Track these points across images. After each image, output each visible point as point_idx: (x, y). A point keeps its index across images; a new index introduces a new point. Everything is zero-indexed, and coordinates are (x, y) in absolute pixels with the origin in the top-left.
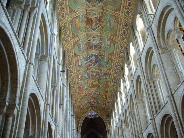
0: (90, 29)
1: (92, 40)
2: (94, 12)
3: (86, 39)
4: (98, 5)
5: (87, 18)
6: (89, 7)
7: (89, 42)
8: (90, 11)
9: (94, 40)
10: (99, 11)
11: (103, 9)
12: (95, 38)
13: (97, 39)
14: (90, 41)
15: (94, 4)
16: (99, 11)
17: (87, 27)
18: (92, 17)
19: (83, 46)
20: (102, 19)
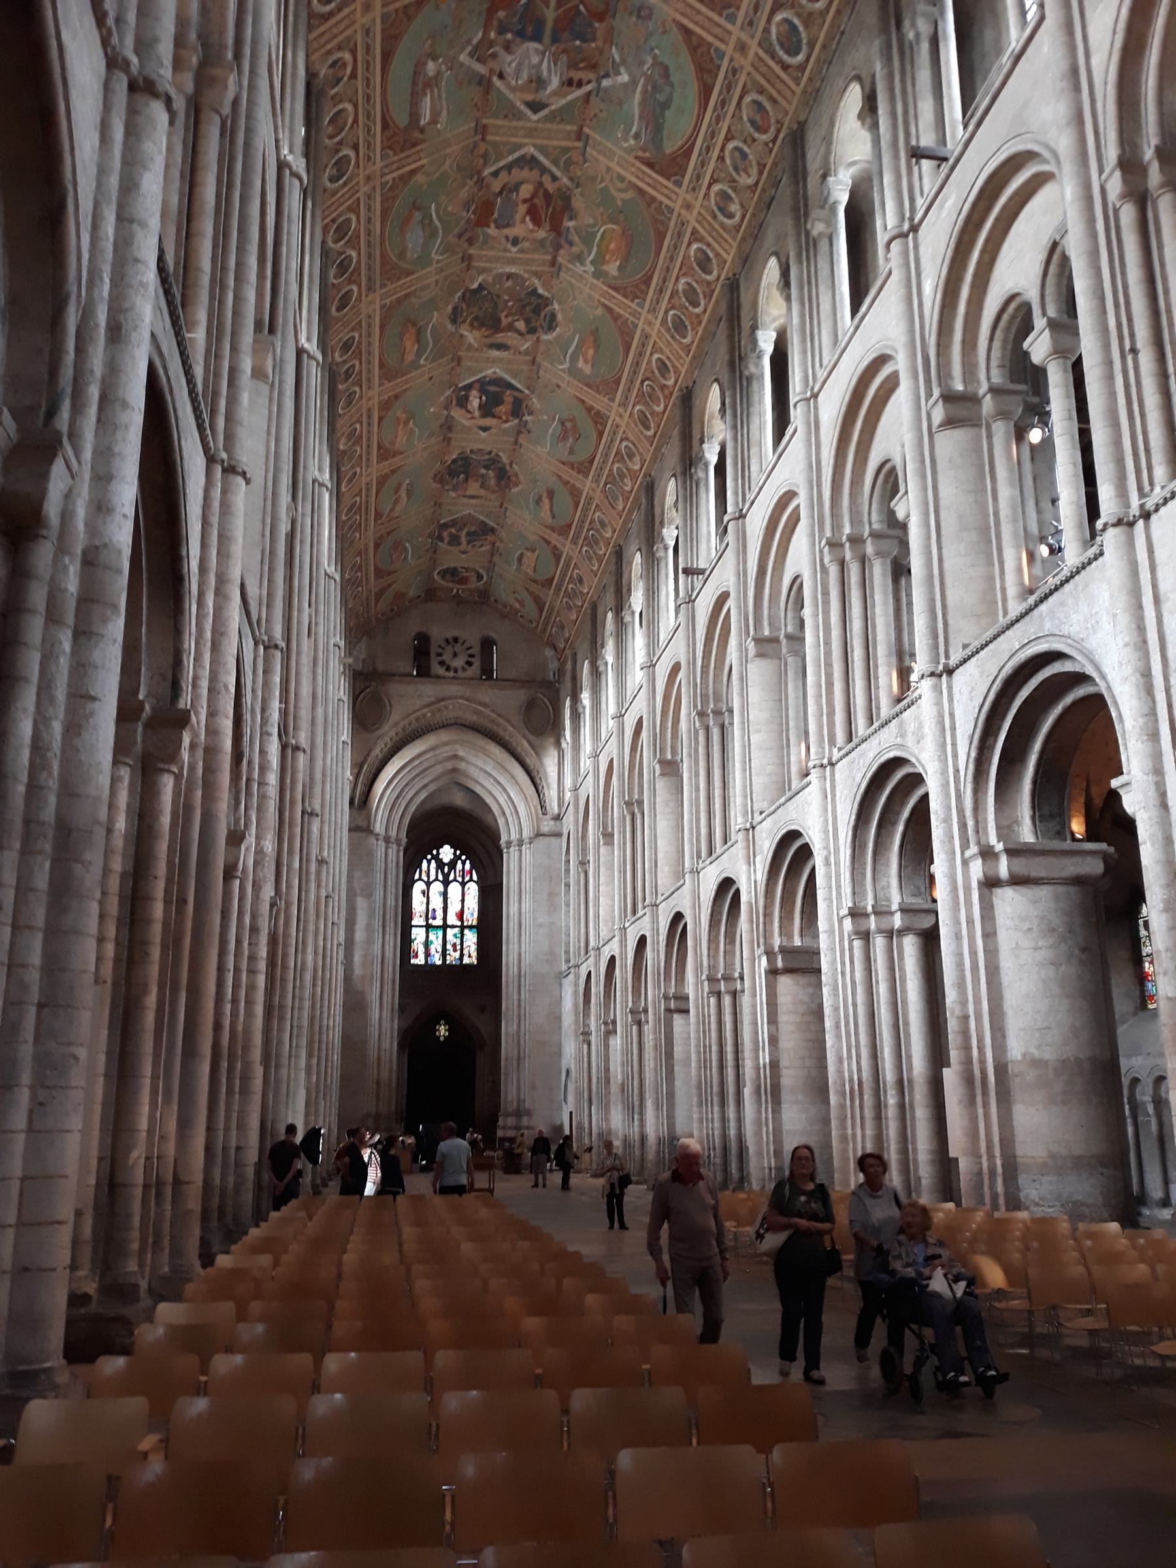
0: (554, 169)
1: (555, 82)
2: (515, 249)
3: (593, 98)
4: (490, 280)
5: (556, 228)
6: (538, 275)
7: (576, 75)
8: (536, 257)
9: (539, 83)
10: (484, 253)
11: (469, 258)
12: (530, 97)
13: (511, 91)
14: (570, 83)
15: (510, 283)
16: (491, 253)
17: (571, 179)
18: (532, 231)
19: (624, 78)
20: (474, 213)
